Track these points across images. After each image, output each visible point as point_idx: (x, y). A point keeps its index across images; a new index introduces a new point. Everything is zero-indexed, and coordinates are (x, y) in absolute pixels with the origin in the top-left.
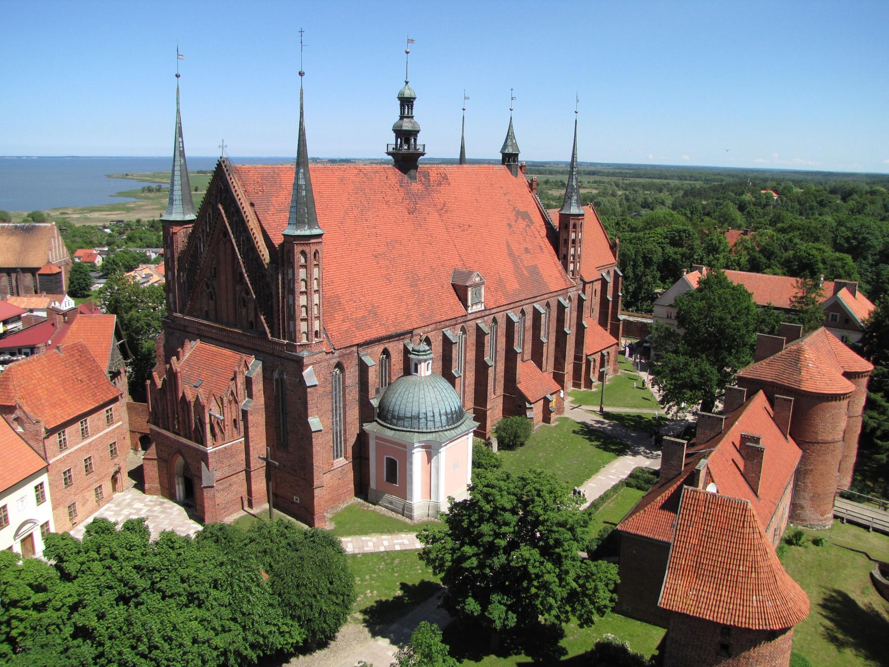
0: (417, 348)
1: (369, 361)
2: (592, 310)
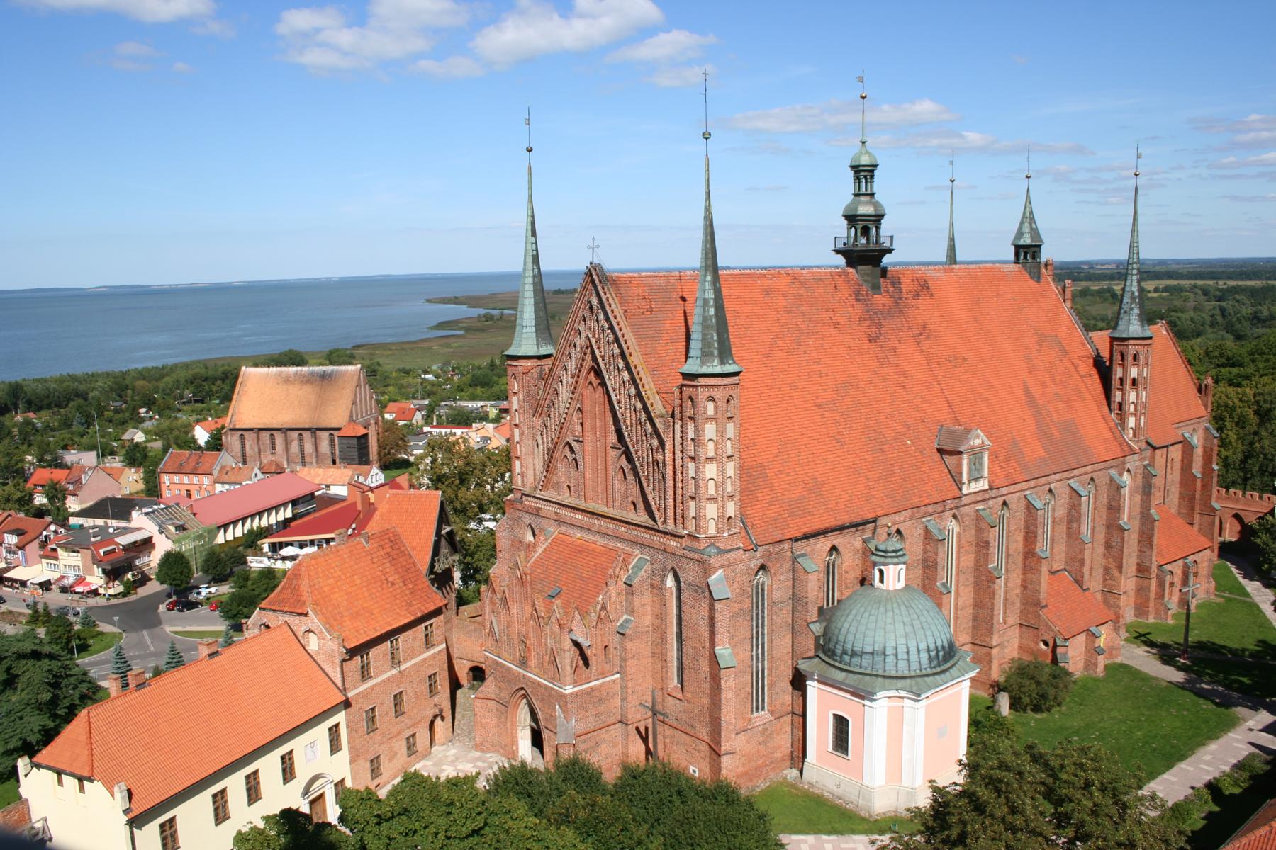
0: (882, 547)
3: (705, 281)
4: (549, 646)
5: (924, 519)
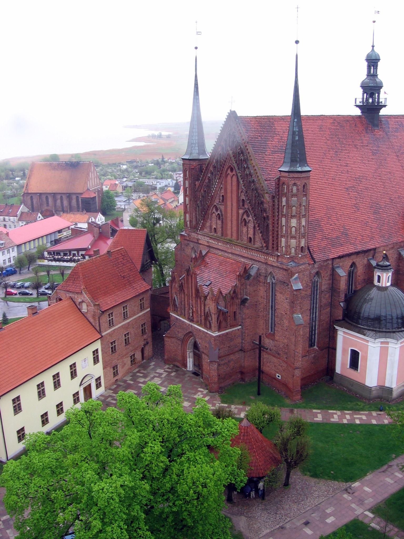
0: (381, 263)
3: (294, 122)
4: (206, 311)
5: (399, 249)
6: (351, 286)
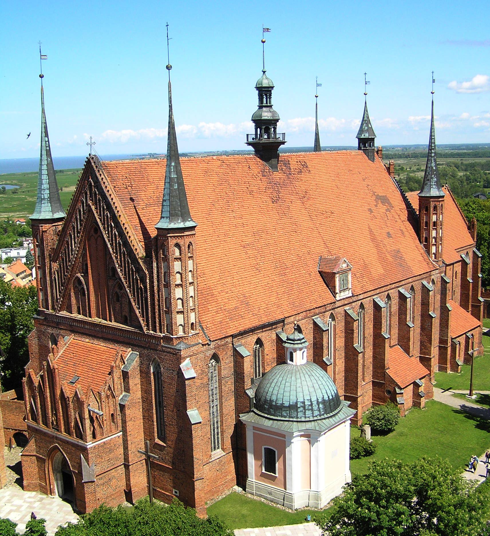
0: (291, 337)
1: (243, 351)
2: (453, 292)
5: (313, 318)
6: (257, 368)
